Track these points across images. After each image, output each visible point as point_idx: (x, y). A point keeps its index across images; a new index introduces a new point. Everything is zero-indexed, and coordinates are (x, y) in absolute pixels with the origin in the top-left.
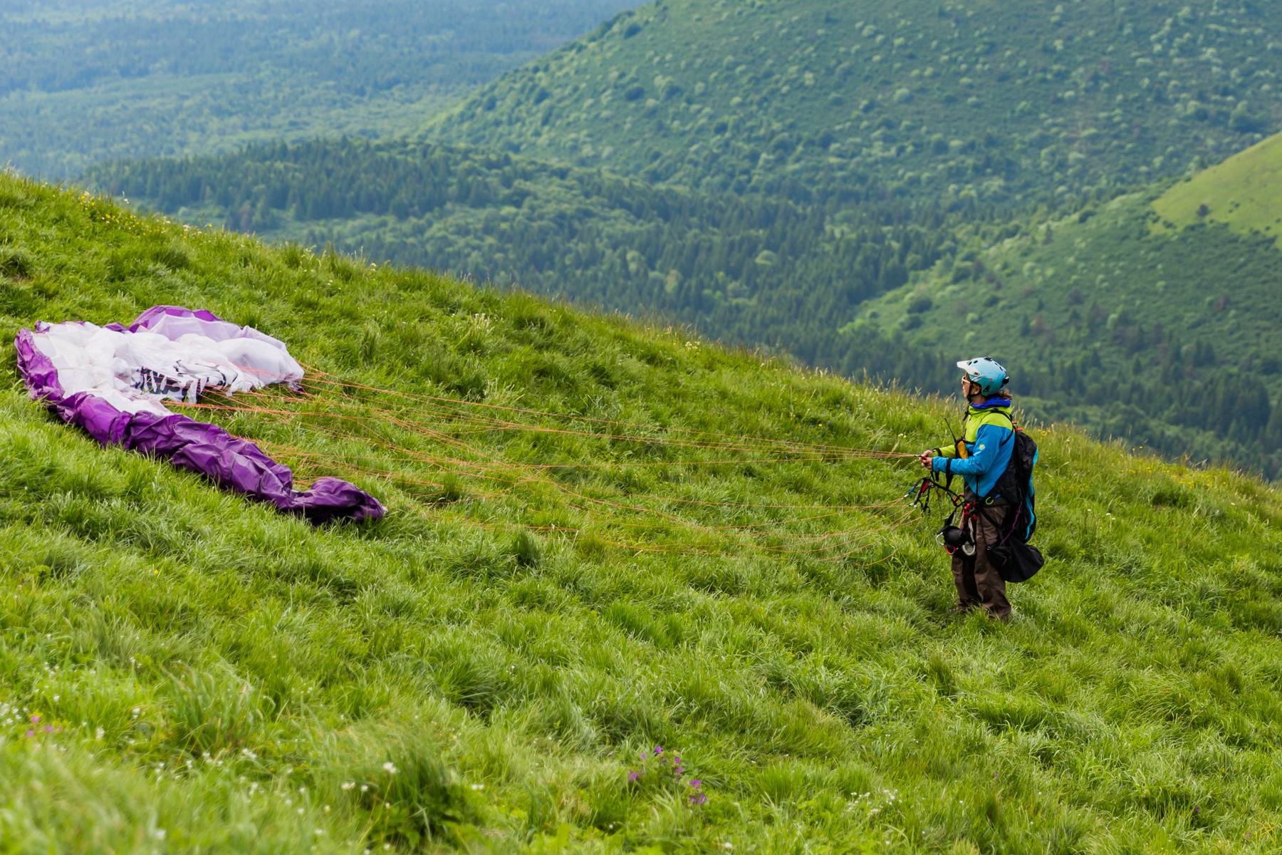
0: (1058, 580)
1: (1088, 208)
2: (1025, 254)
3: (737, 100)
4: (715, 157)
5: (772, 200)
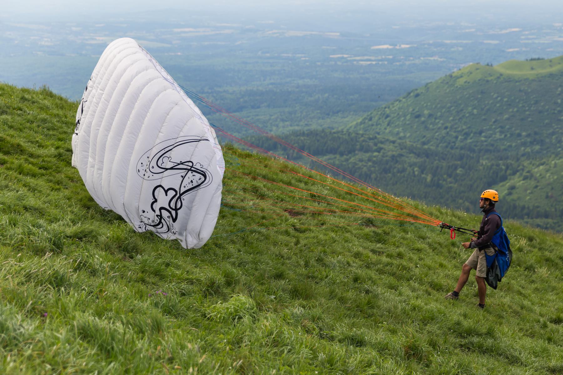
3: (451, 118)
4: (444, 137)
5: (463, 152)
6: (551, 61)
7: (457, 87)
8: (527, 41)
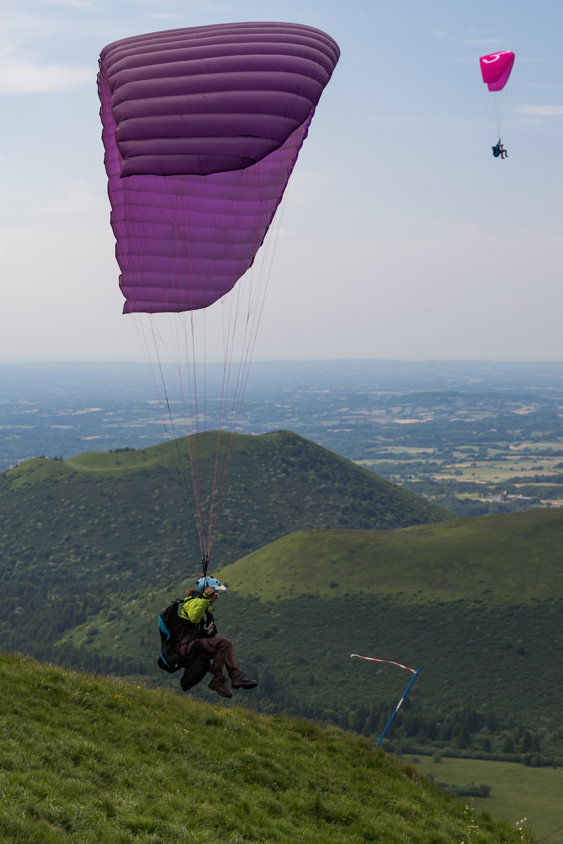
0: (162, 762)
1: (171, 585)
2: (142, 607)
3: (5, 536)
5: (22, 583)
6: (144, 452)
7: (13, 491)
8: (111, 426)
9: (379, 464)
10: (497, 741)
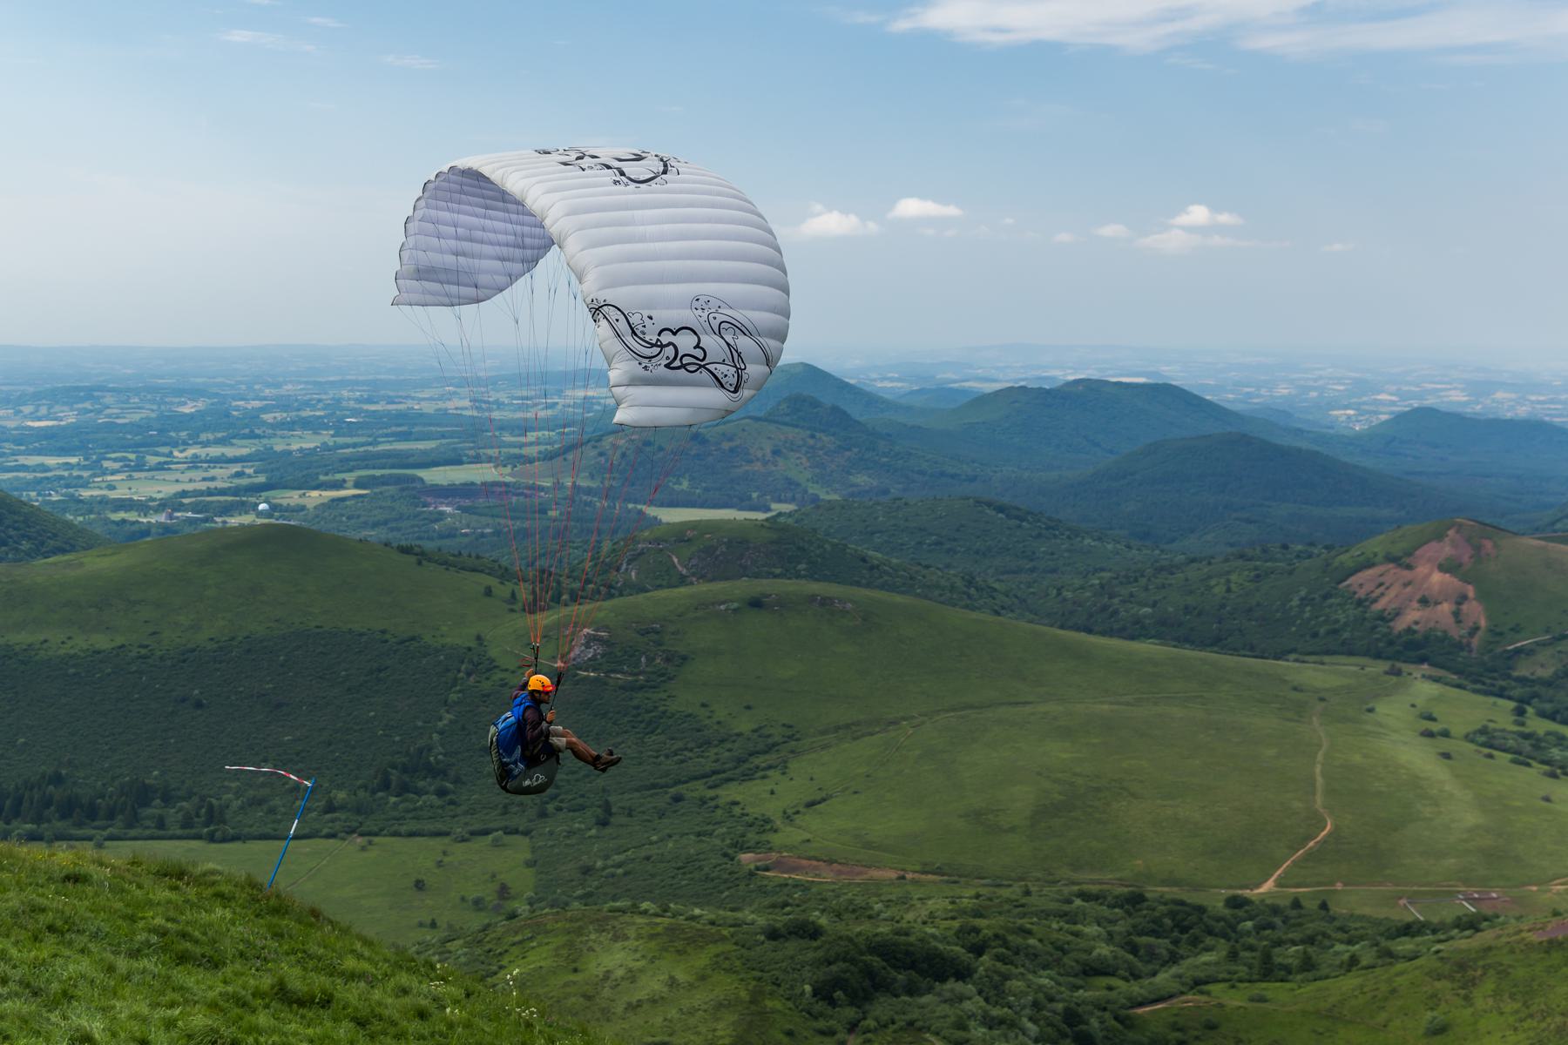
9: (9, 479)
10: (173, 815)
